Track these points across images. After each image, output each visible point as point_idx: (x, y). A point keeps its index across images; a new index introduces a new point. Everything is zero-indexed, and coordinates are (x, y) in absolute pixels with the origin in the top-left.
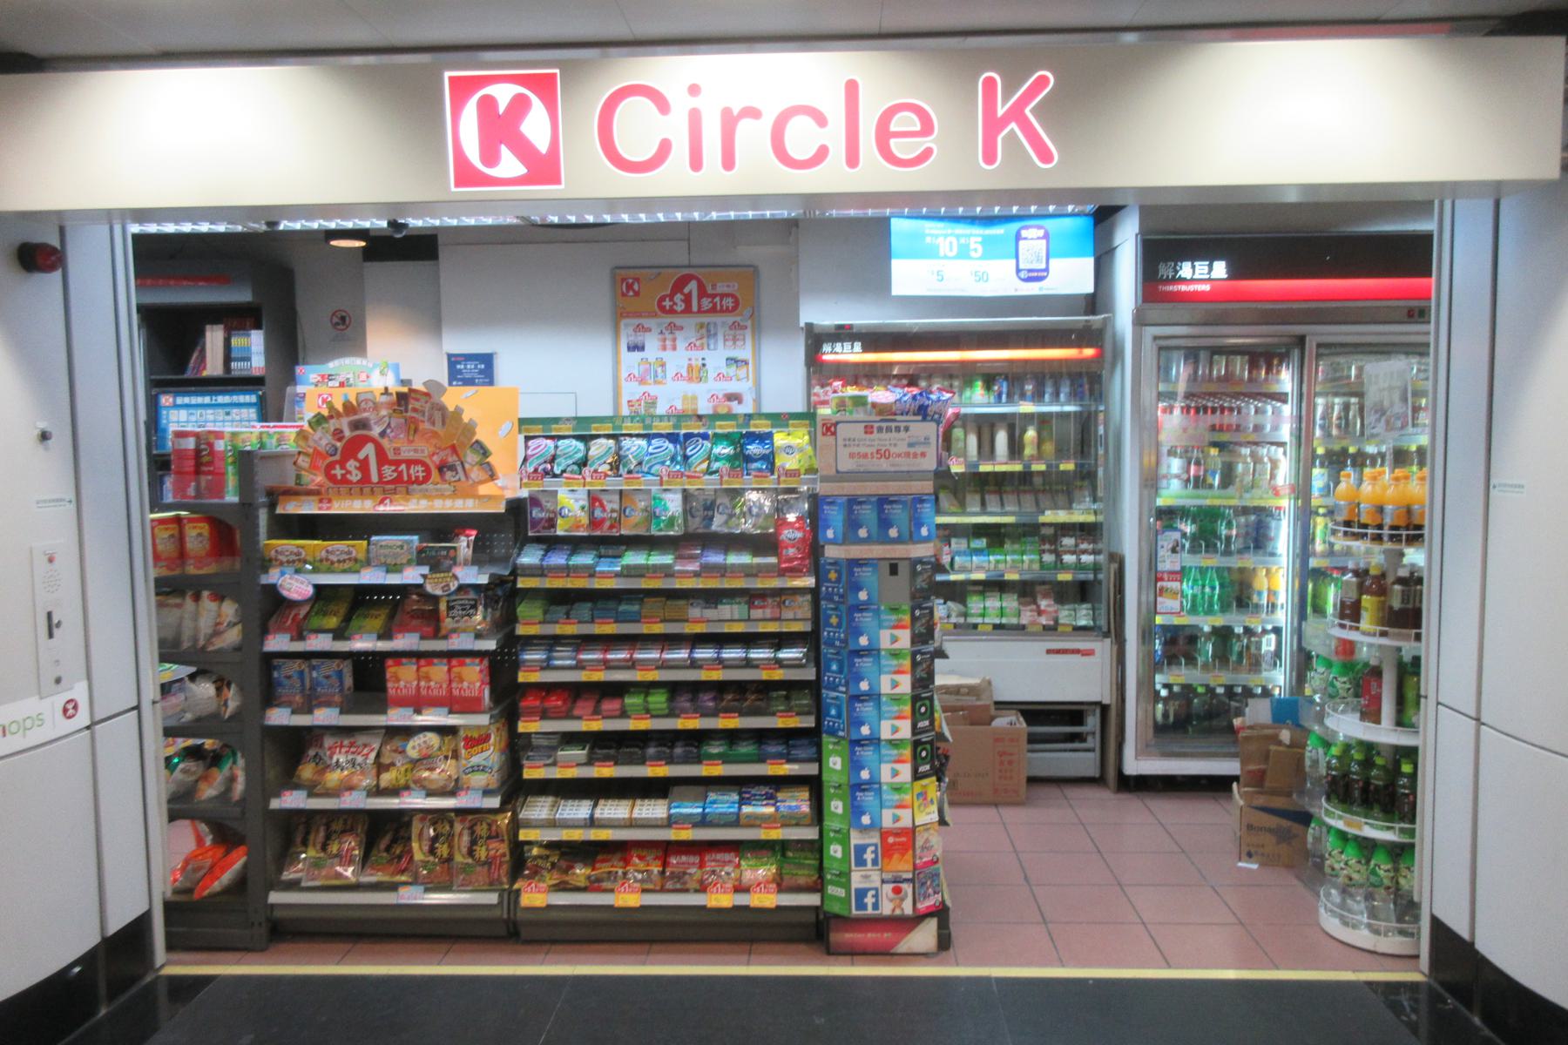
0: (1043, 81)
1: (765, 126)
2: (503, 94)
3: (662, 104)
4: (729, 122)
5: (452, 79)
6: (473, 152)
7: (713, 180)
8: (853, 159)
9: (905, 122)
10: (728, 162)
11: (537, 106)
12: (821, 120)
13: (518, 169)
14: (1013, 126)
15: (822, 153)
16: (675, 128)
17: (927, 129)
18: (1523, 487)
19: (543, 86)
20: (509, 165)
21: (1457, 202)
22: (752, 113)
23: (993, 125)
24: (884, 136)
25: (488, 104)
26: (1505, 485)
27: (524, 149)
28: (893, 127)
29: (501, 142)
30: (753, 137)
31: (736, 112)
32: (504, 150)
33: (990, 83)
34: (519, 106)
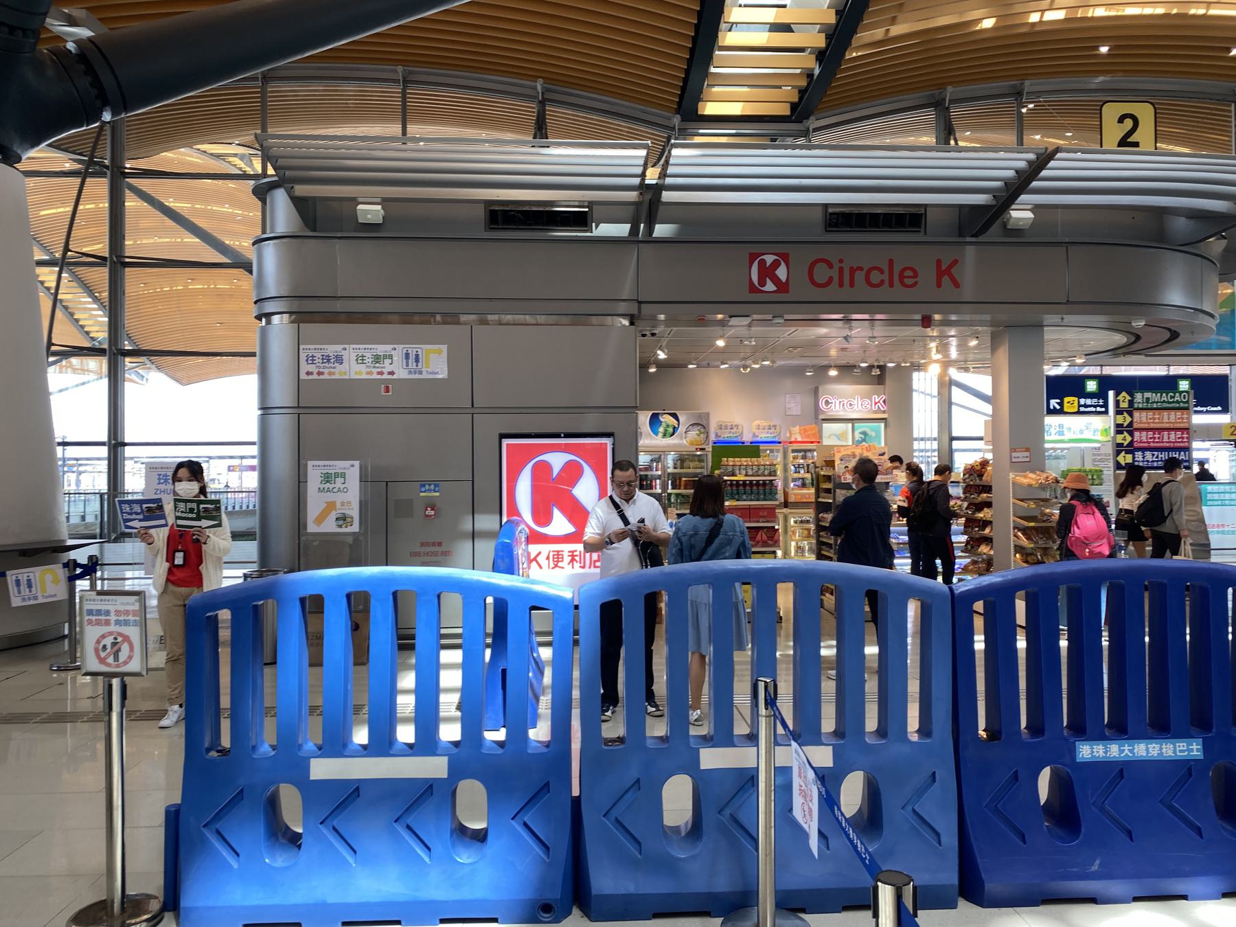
2: (769, 259)
4: (853, 271)
6: (755, 278)
11: (783, 266)
15: (882, 282)
20: (770, 286)
22: (860, 269)
25: (762, 262)
27: (776, 281)
29: (767, 276)
31: (855, 267)
32: (768, 280)
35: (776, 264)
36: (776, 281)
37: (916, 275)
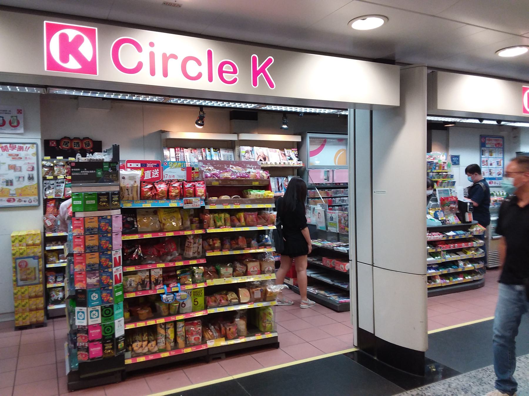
0: (270, 60)
1: (179, 61)
3: (139, 48)
4: (166, 59)
5: (47, 23)
6: (56, 55)
7: (158, 81)
8: (210, 79)
10: (165, 74)
11: (86, 40)
12: (199, 63)
13: (77, 66)
14: (262, 74)
15: (199, 76)
16: (144, 57)
17: (235, 72)
18: (385, 192)
19: (91, 34)
20: (73, 64)
21: (356, 110)
22: (174, 57)
23: (256, 73)
24: (221, 72)
25: (64, 38)
26: (378, 192)
27: (80, 58)
28: (224, 69)
30: (174, 66)
31: (168, 56)
32: (71, 57)
33: (254, 58)
34: (79, 40)
37: (235, 72)
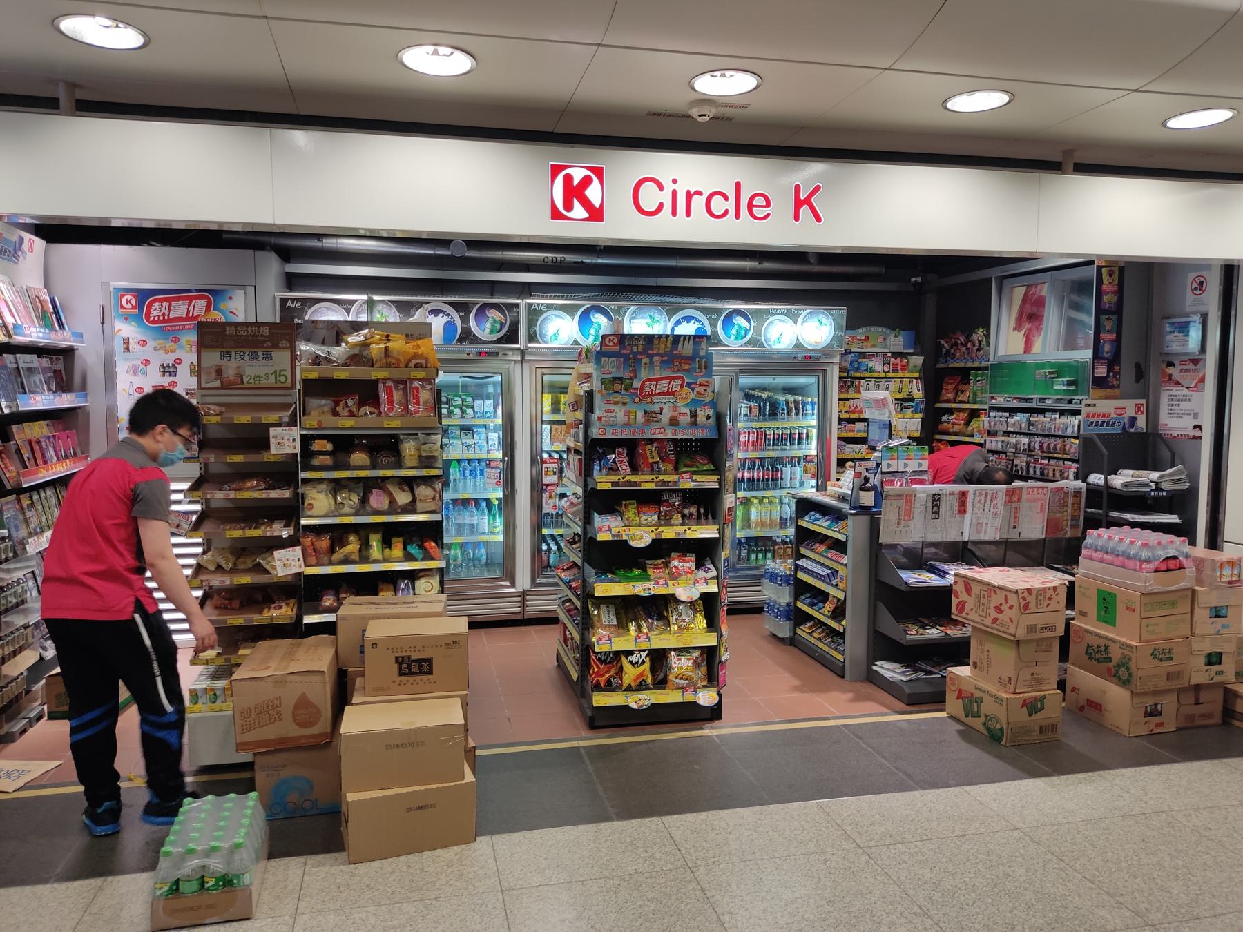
2: (578, 174)
4: (689, 196)
9: (759, 201)
12: (726, 198)
15: (726, 212)
22: (699, 193)
24: (751, 206)
27: (587, 204)
32: (576, 203)
35: (586, 182)
36: (587, 204)
37: (768, 205)
